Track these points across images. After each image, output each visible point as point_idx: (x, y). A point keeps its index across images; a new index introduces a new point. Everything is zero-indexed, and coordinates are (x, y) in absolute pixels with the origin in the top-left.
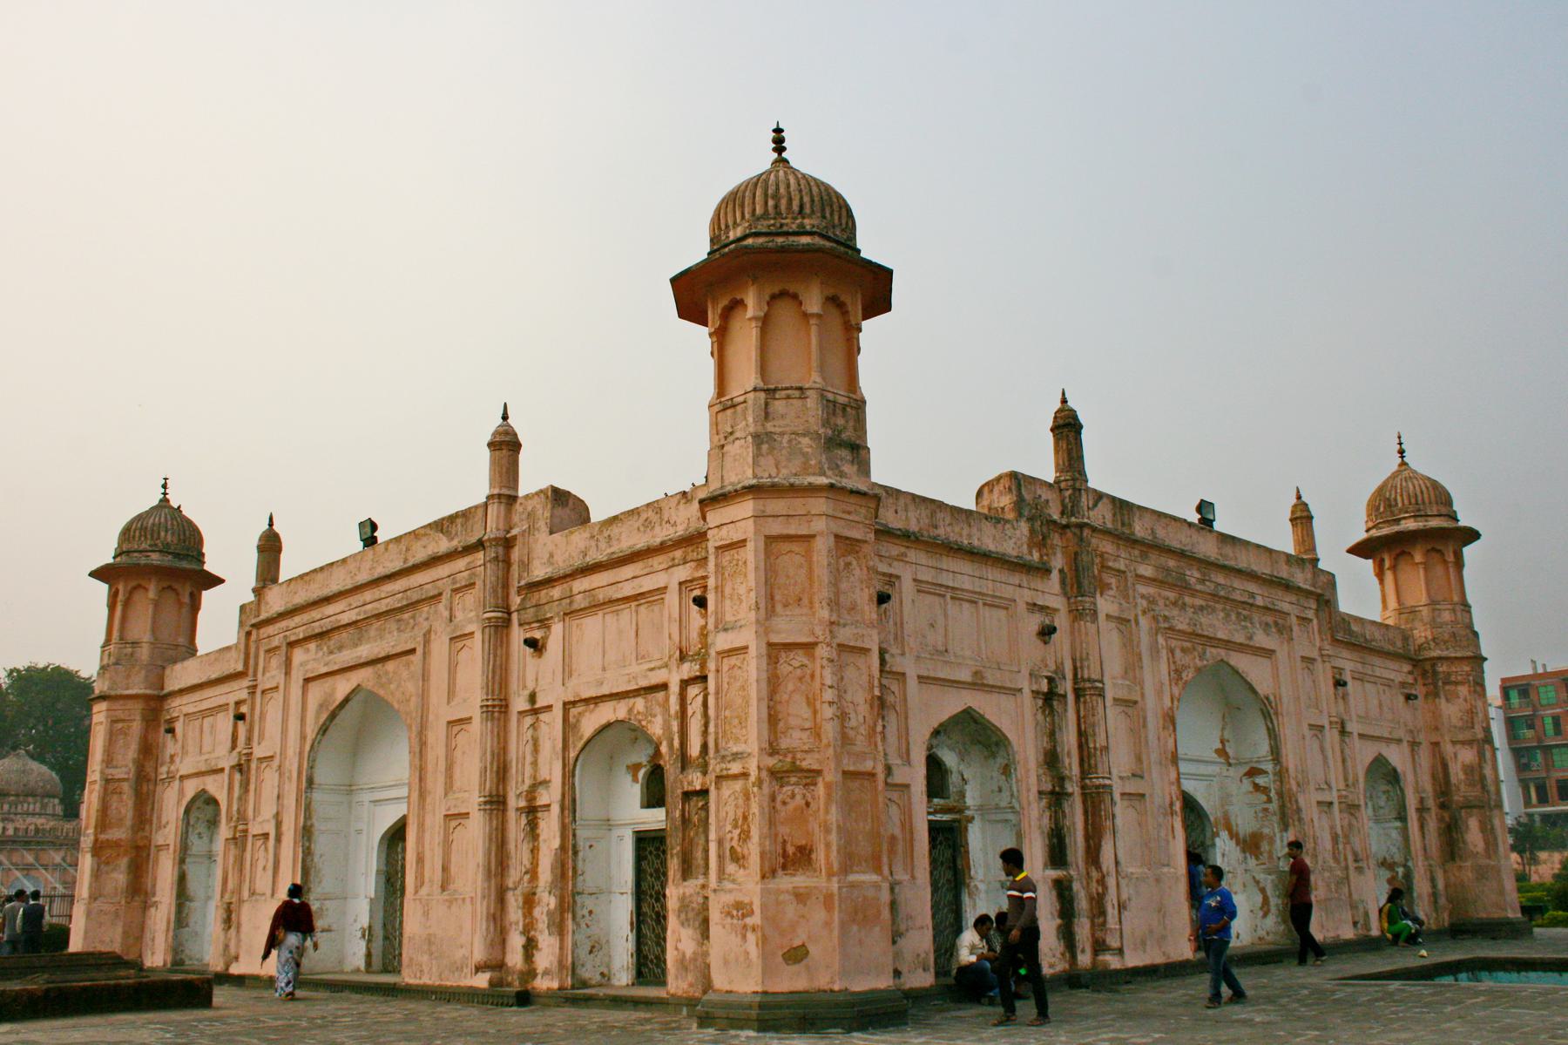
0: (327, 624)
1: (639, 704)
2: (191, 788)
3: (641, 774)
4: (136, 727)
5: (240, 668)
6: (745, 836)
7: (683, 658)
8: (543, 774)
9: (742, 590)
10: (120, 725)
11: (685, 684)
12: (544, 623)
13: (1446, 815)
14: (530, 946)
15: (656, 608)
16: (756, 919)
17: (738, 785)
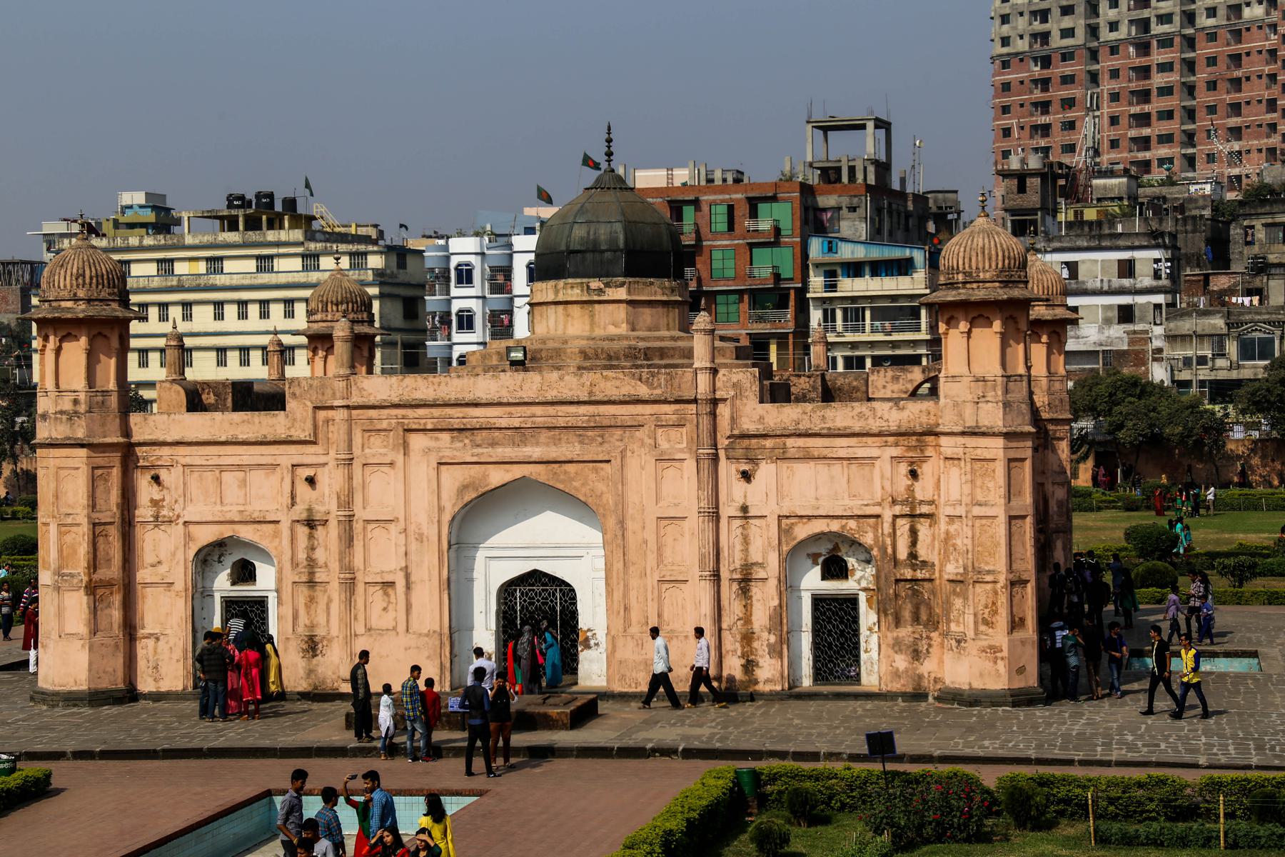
0: (474, 423)
1: (852, 524)
2: (206, 535)
3: (821, 560)
4: (116, 473)
5: (302, 436)
6: (995, 612)
7: (894, 502)
8: (755, 556)
9: (991, 485)
10: (99, 472)
11: (895, 517)
12: (753, 461)
13: (1042, 538)
14: (749, 666)
15: (867, 468)
16: (1005, 654)
17: (989, 587)
